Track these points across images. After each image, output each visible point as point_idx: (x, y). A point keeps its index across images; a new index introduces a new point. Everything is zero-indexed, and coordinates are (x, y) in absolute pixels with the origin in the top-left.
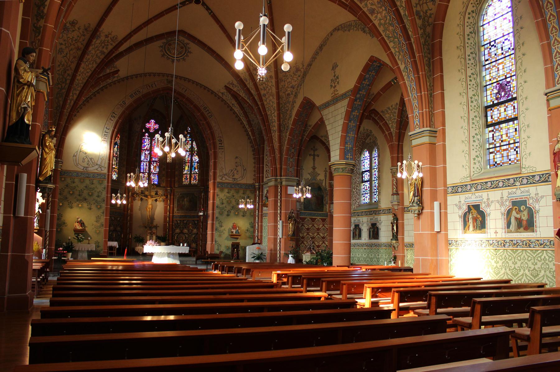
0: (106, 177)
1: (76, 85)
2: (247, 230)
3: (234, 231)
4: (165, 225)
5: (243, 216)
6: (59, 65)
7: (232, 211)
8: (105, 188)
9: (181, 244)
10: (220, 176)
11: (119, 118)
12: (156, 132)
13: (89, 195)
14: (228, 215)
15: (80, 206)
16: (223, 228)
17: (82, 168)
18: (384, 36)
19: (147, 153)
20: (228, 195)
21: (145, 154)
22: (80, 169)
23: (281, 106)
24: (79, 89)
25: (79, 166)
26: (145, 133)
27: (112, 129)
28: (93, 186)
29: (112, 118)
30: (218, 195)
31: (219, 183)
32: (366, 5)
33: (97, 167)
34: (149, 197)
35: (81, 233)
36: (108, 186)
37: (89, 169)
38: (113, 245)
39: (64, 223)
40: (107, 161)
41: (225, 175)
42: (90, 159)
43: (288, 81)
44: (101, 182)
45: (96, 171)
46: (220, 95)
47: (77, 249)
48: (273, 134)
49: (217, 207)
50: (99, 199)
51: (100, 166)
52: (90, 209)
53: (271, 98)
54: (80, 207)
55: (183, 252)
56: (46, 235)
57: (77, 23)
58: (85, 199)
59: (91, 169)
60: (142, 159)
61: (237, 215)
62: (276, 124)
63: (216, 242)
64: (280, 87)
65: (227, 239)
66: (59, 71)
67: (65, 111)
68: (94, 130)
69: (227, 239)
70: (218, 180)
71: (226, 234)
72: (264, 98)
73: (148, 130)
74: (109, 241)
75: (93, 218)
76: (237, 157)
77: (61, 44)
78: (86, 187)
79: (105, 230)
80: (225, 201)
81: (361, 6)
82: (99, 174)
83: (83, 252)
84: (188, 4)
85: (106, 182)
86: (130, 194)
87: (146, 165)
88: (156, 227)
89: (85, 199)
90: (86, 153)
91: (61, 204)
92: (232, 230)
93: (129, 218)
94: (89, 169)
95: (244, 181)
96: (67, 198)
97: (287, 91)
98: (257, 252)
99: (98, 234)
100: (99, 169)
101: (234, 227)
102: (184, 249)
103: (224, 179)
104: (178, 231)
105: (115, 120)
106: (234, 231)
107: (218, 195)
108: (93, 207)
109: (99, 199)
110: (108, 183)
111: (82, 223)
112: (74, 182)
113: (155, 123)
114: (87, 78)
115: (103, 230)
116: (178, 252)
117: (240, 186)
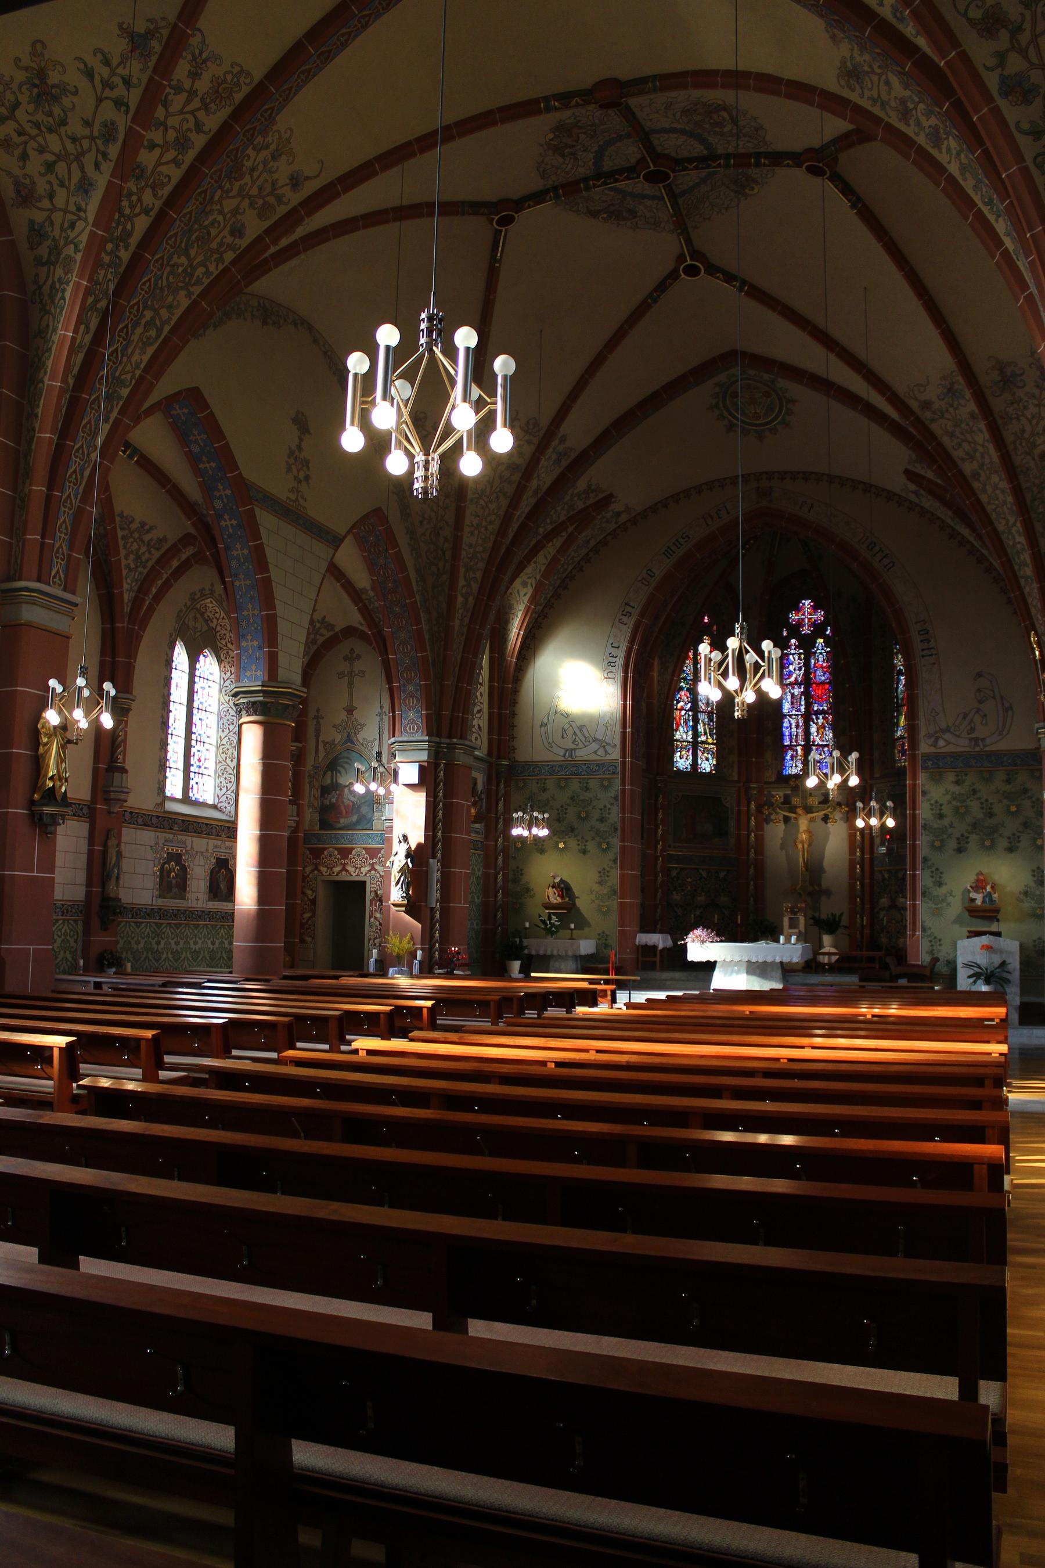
0: (619, 769)
1: (471, 559)
2: (1026, 893)
3: (979, 898)
4: (852, 886)
5: (1010, 850)
6: (421, 522)
7: (974, 838)
8: (616, 798)
9: (782, 938)
10: (929, 736)
11: (642, 615)
12: (818, 629)
13: (580, 817)
14: (960, 850)
15: (561, 845)
16: (943, 890)
17: (562, 752)
18: (980, 205)
19: (796, 691)
20: (957, 789)
21: (793, 695)
22: (557, 755)
23: (1028, 497)
24: (481, 565)
25: (555, 749)
26: (788, 639)
27: (624, 646)
28: (587, 795)
29: (625, 619)
30: (924, 793)
31: (927, 757)
32: (918, 123)
33: (595, 746)
34: (800, 811)
36: (623, 791)
37: (578, 753)
38: (650, 943)
39: (528, 890)
40: (618, 729)
41: (944, 731)
42: (579, 728)
43: (1028, 414)
44: (606, 783)
46: (913, 498)
47: (541, 953)
48: (1027, 590)
49: (924, 827)
50: (603, 827)
51: (603, 744)
52: (584, 852)
53: (995, 478)
54: (561, 850)
55: (786, 960)
56: (432, 917)
57: (426, 418)
58: (573, 830)
59: (585, 753)
60: (785, 710)
61: (991, 848)
62: (1026, 557)
63: (924, 930)
64: (1009, 438)
65: (958, 921)
66: (424, 534)
67: (457, 623)
68: (583, 655)
69: (958, 921)
70: (924, 747)
71: (955, 907)
72: (976, 485)
73: (795, 630)
74: (643, 930)
75: (593, 876)
76: (979, 675)
78: (572, 798)
80: (946, 810)
81: (909, 131)
82: (602, 765)
83: (560, 957)
84: (671, 284)
85: (618, 781)
86: (753, 806)
87: (797, 726)
88: (828, 893)
89: (573, 830)
90: (567, 715)
92: (973, 895)
93: (752, 871)
94: (578, 753)
95: (1003, 746)
97: (1035, 446)
98: (983, 959)
99: (605, 914)
100: (601, 752)
101: (979, 885)
102: (788, 949)
103: (941, 743)
104: (884, 901)
105: (631, 622)
106: (979, 898)
107: (924, 793)
108: (591, 846)
109: (603, 827)
110: (623, 783)
111: (564, 888)
112: (544, 790)
113: (815, 608)
114: (492, 538)
115: (615, 903)
116: (778, 960)
117: (997, 758)
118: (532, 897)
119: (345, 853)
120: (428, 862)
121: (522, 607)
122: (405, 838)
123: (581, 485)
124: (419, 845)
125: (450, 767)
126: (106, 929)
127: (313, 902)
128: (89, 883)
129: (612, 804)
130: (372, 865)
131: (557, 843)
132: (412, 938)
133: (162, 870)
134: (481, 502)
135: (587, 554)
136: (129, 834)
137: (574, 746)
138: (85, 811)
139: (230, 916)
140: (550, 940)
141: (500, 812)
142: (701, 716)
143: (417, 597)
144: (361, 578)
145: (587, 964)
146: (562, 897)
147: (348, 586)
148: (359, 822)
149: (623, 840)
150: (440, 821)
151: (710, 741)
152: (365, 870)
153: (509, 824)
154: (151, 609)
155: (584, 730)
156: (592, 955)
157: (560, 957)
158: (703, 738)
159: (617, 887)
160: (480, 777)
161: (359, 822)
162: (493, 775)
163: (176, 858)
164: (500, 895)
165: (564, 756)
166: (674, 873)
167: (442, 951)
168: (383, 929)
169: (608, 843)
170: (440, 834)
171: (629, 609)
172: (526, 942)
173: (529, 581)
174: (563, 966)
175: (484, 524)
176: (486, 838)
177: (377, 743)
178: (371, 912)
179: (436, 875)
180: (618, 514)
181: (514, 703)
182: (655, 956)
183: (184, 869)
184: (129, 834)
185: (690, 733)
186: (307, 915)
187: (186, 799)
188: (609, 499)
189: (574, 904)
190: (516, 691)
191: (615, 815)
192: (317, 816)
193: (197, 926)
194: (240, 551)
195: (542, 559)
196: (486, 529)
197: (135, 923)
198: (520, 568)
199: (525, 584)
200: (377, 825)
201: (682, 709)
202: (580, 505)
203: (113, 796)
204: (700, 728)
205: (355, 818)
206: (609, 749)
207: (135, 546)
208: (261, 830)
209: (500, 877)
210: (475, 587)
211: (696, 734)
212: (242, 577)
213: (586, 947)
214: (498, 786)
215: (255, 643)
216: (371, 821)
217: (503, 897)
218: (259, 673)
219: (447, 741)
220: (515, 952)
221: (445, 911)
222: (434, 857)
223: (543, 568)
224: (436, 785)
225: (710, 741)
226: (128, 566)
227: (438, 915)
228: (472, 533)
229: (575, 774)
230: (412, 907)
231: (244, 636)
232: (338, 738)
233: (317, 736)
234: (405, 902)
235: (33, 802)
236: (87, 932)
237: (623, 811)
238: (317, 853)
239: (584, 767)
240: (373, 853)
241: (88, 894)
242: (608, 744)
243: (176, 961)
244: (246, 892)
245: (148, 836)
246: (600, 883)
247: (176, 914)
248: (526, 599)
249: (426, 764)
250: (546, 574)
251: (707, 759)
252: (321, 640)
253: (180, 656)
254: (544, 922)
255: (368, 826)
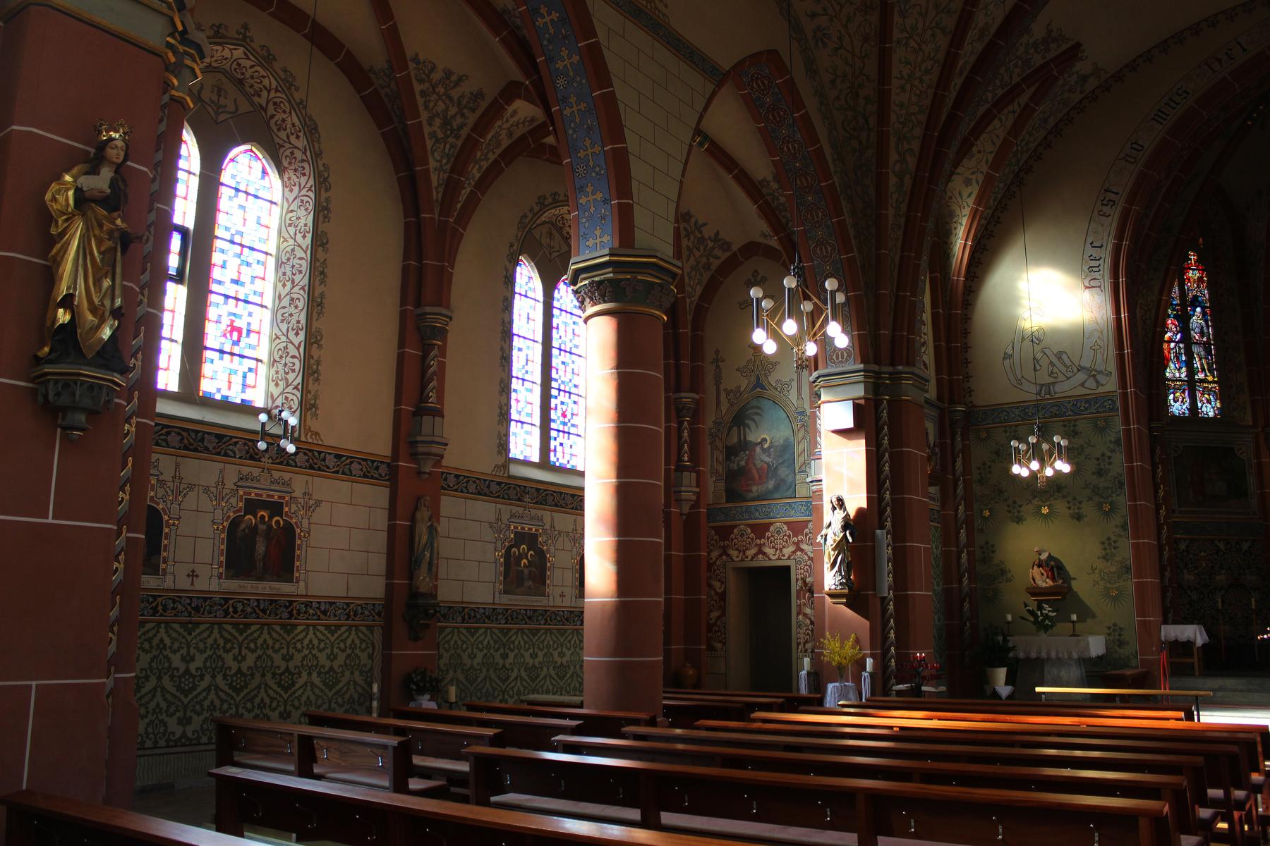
0: (1118, 404)
8: (1117, 442)
15: (1045, 510)
17: (1033, 389)
22: (1028, 393)
24: (918, 132)
25: (1026, 386)
27: (1110, 244)
33: (1081, 377)
35: (1060, 596)
37: (1058, 388)
39: (1003, 572)
40: (1112, 352)
45: (1082, 391)
47: (1033, 655)
51: (1093, 373)
52: (1078, 517)
56: (884, 611)
59: (1068, 387)
74: (1165, 622)
77: (813, 16)
79: (1140, 587)
82: (1094, 400)
83: (1060, 662)
85: (1118, 421)
91: (987, 513)
94: (1058, 388)
96: (1001, 492)
100: (1091, 383)
105: (1116, 213)
108: (1088, 509)
110: (1126, 421)
111: (1054, 567)
115: (1129, 584)
118: (1009, 580)
119: (761, 530)
120: (874, 534)
121: (966, 211)
122: (841, 503)
123: (1038, 30)
124: (860, 511)
125: (895, 404)
126: (416, 639)
127: (723, 596)
128: (390, 574)
129: (1113, 451)
130: (797, 544)
131: (1039, 508)
132: (857, 641)
133: (507, 556)
134: (912, 43)
135: (1045, 138)
136: (449, 504)
137: (1051, 380)
138: (383, 470)
139: (576, 616)
140: (1043, 636)
141: (958, 474)
142: (1195, 349)
143: (836, 179)
144: (760, 166)
145: (1096, 672)
146: (1053, 579)
147: (743, 178)
148: (777, 488)
149: (1133, 498)
150: (887, 477)
151: (1210, 378)
152: (787, 551)
153: (1008, 457)
154: (472, 203)
155: (1064, 356)
156: (1100, 658)
157: (1060, 662)
158: (1201, 376)
159: (1130, 562)
160: (930, 427)
161: (777, 488)
162: (946, 426)
163: (531, 540)
164: (965, 581)
165: (1039, 393)
166: (1183, 546)
167: (899, 657)
168: (816, 629)
169: (1111, 504)
170: (888, 495)
171: (1112, 196)
172: (1012, 641)
173: (974, 177)
174: (1063, 673)
175: (918, 74)
176: (943, 506)
177: (794, 384)
178: (799, 606)
179: (886, 552)
180: (1084, 79)
181: (966, 333)
182: (1191, 655)
183: (541, 555)
184: (449, 504)
185: (1184, 369)
186: (715, 614)
187: (545, 463)
188: (1074, 52)
189: (1070, 588)
190: (967, 318)
191: (1118, 465)
192: (722, 485)
193: (562, 632)
194: (567, 60)
195: (986, 146)
196: (921, 81)
197: (327, 627)
198: (965, 149)
199: (968, 182)
200: (801, 491)
201: (1171, 341)
202: (1038, 60)
203: (421, 449)
204: (1197, 363)
205: (771, 484)
206: (1099, 377)
207: (441, 106)
208: (618, 476)
209: (964, 556)
210: (912, 162)
211: (1191, 371)
212: (573, 100)
213: (1096, 646)
214: (953, 439)
215: (599, 196)
216: (792, 487)
217: (970, 582)
218: (606, 239)
219: (890, 369)
220: (999, 655)
221: (901, 601)
222: (882, 527)
223: (991, 157)
224: (879, 431)
225: (1210, 378)
226: (433, 134)
227: (891, 607)
228: (902, 88)
229: (1056, 416)
230: (857, 594)
231: (582, 189)
232: (744, 384)
233: (718, 384)
234: (846, 591)
235: (38, 360)
236: (387, 643)
237: (1129, 458)
238: (725, 533)
239: (1069, 406)
240: (797, 528)
241: (390, 588)
242: (1101, 372)
243: (533, 680)
244: (600, 574)
245: (485, 509)
246: (1105, 558)
247: (531, 616)
248: (971, 201)
249: (862, 402)
250: (995, 165)
251: (1209, 402)
252: (716, 263)
253: (527, 278)
254: (1032, 613)
255: (789, 493)
